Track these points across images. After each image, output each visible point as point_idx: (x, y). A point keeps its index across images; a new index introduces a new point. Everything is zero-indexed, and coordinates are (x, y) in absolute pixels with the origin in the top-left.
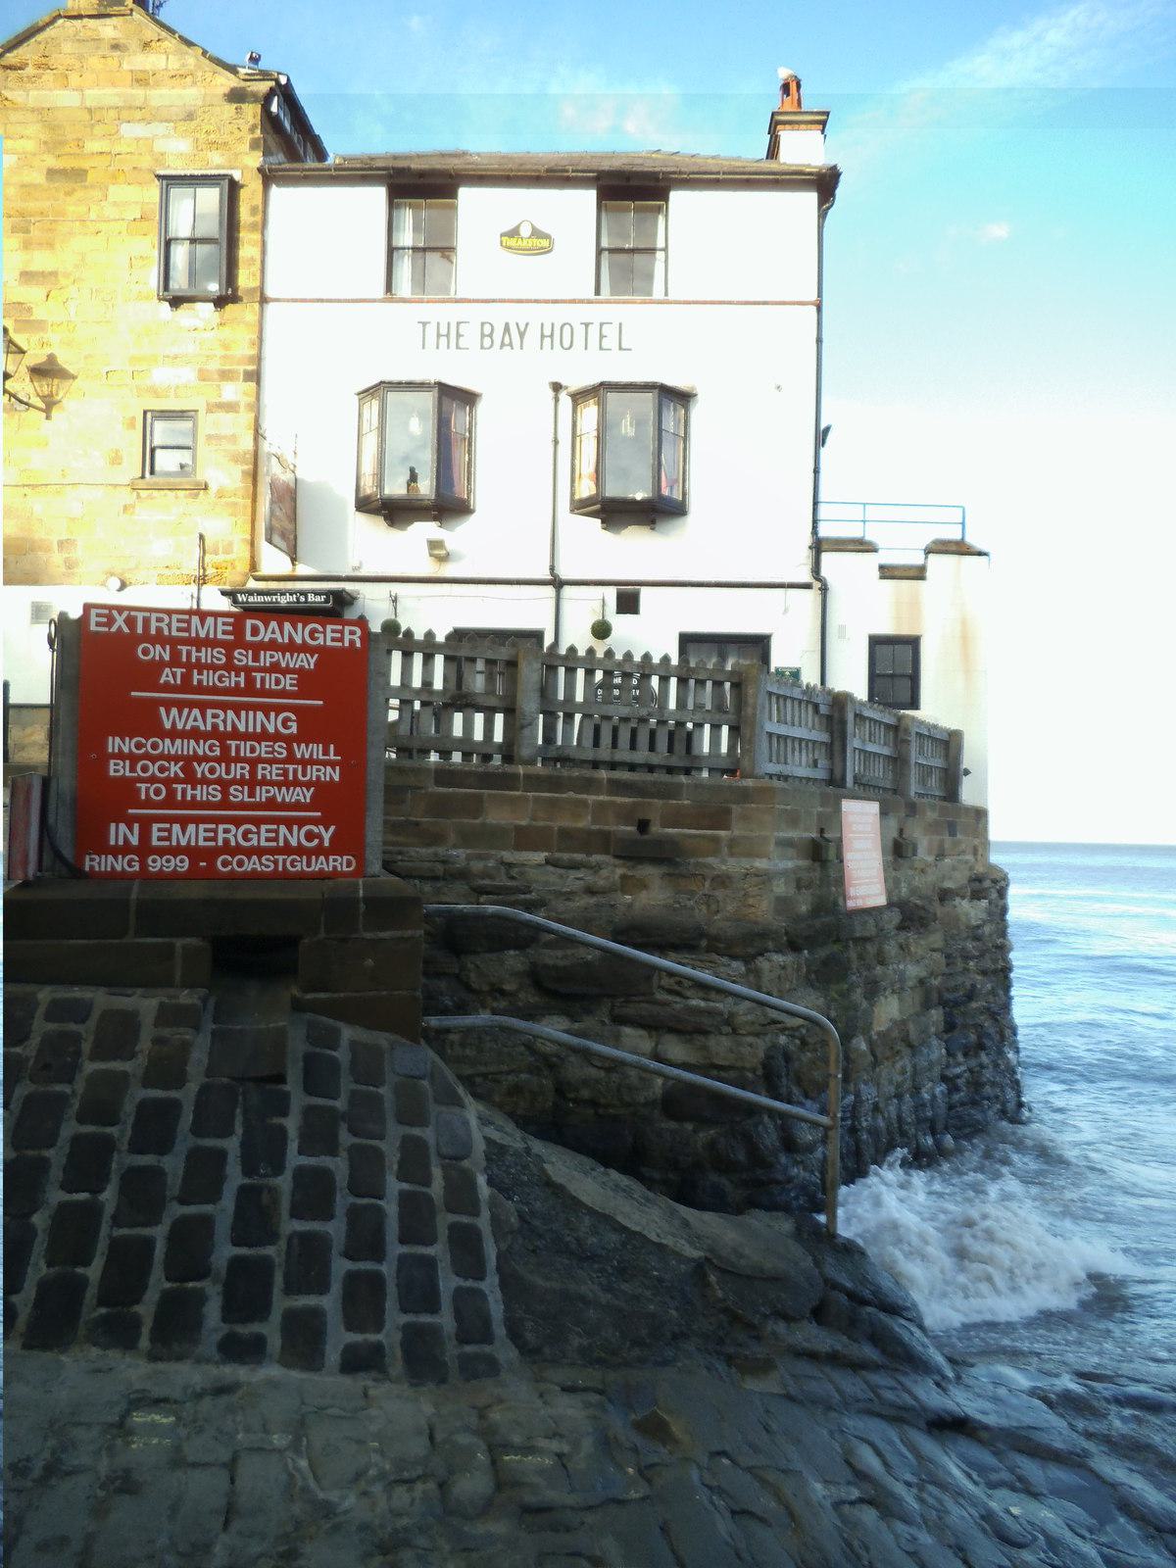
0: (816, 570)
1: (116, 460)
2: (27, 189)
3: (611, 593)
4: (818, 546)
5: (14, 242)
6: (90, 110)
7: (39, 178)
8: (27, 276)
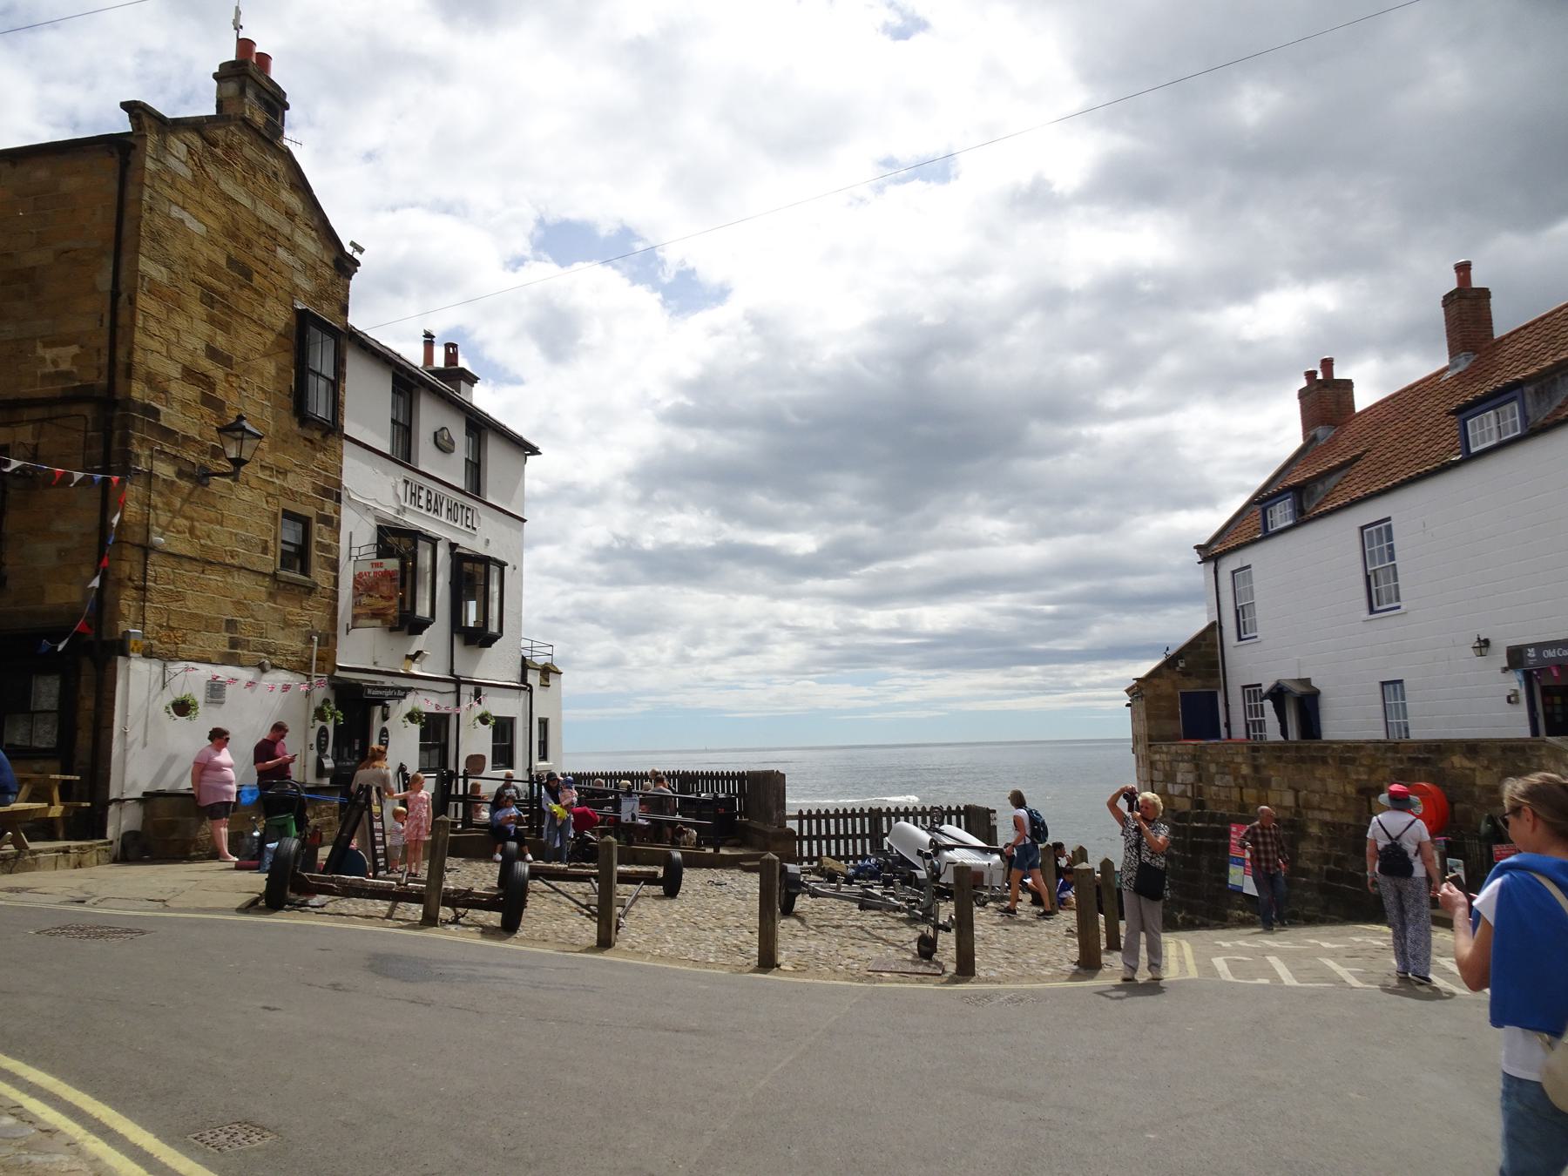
0: (524, 678)
1: (265, 550)
2: (213, 269)
3: (471, 689)
4: (525, 665)
5: (198, 309)
6: (258, 220)
7: (223, 262)
8: (213, 353)
